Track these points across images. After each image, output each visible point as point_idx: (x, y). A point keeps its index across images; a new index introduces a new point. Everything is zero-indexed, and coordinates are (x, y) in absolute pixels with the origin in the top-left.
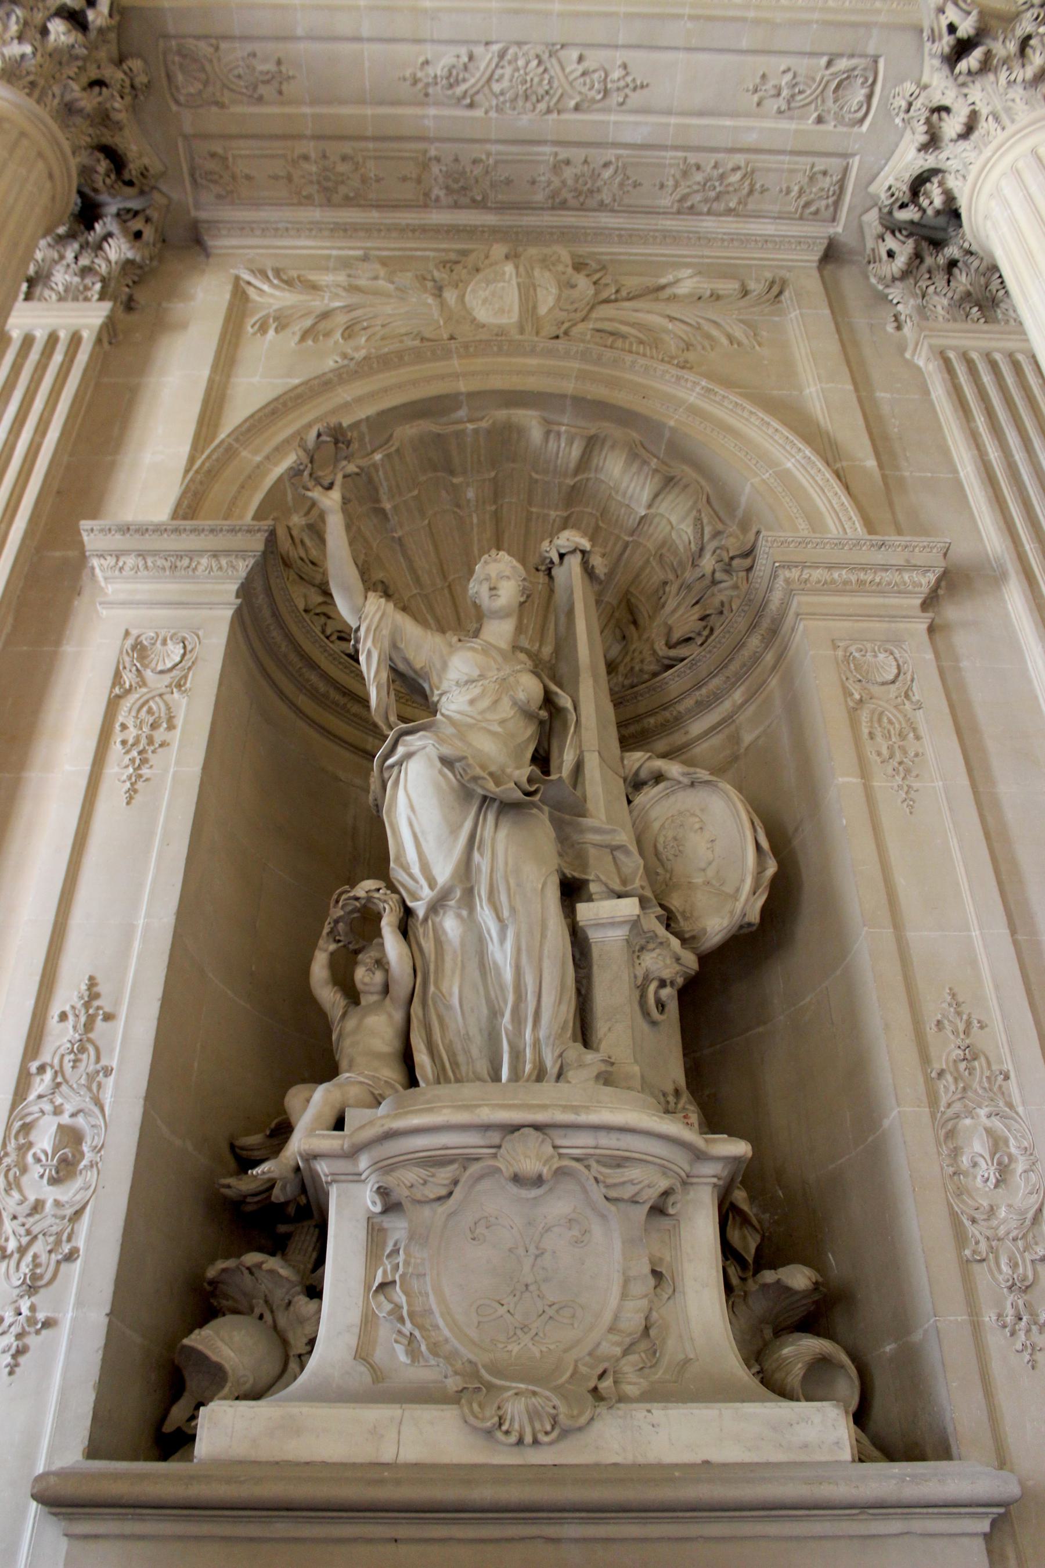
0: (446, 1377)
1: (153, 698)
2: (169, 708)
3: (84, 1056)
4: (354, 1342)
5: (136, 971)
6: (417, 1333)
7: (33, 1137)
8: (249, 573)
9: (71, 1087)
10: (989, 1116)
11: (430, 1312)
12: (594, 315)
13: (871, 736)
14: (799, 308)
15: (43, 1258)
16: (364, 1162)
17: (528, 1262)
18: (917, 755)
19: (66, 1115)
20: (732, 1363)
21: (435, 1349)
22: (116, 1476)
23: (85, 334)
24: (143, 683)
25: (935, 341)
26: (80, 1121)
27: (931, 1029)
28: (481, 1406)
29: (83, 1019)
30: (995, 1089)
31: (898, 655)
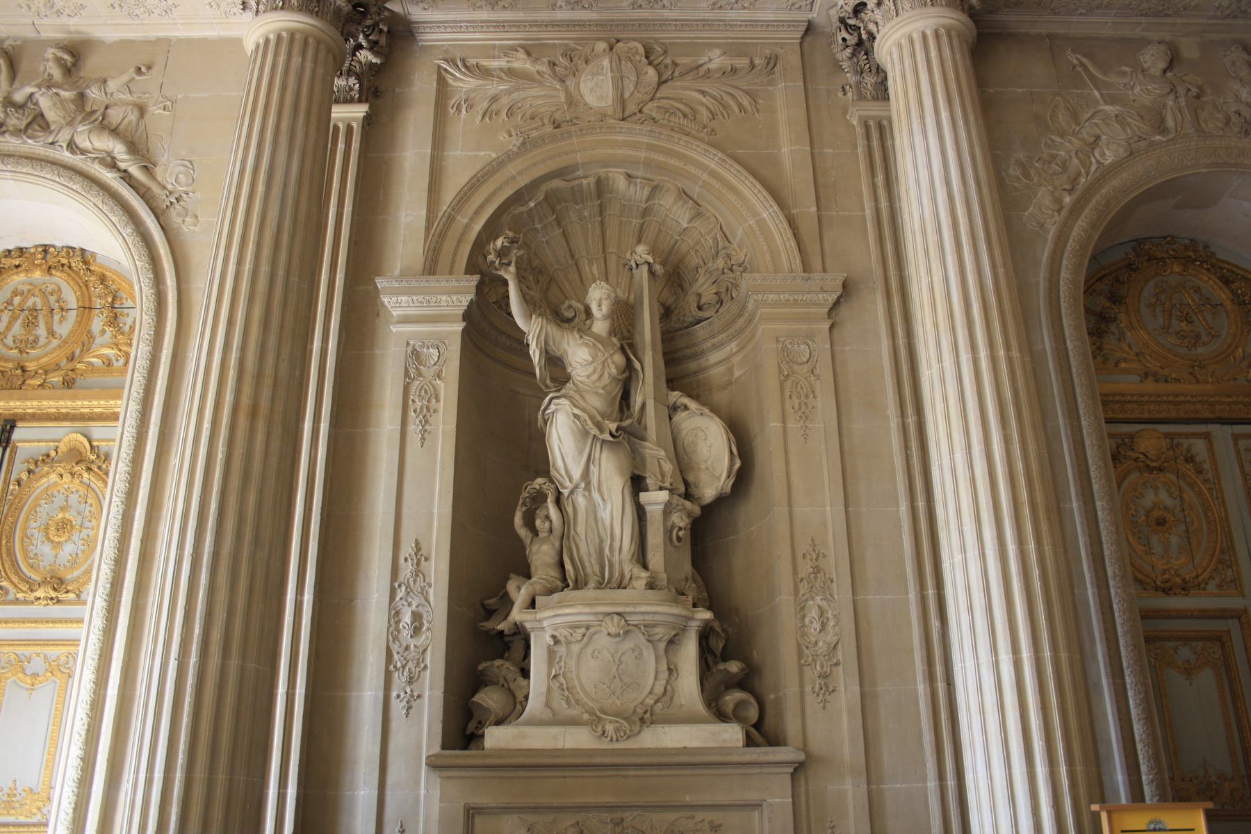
4: (544, 699)
8: (469, 307)
12: (658, 95)
13: (790, 397)
17: (614, 668)
20: (699, 706)
21: (577, 702)
22: (456, 756)
23: (354, 125)
24: (420, 375)
25: (862, 113)
27: (799, 556)
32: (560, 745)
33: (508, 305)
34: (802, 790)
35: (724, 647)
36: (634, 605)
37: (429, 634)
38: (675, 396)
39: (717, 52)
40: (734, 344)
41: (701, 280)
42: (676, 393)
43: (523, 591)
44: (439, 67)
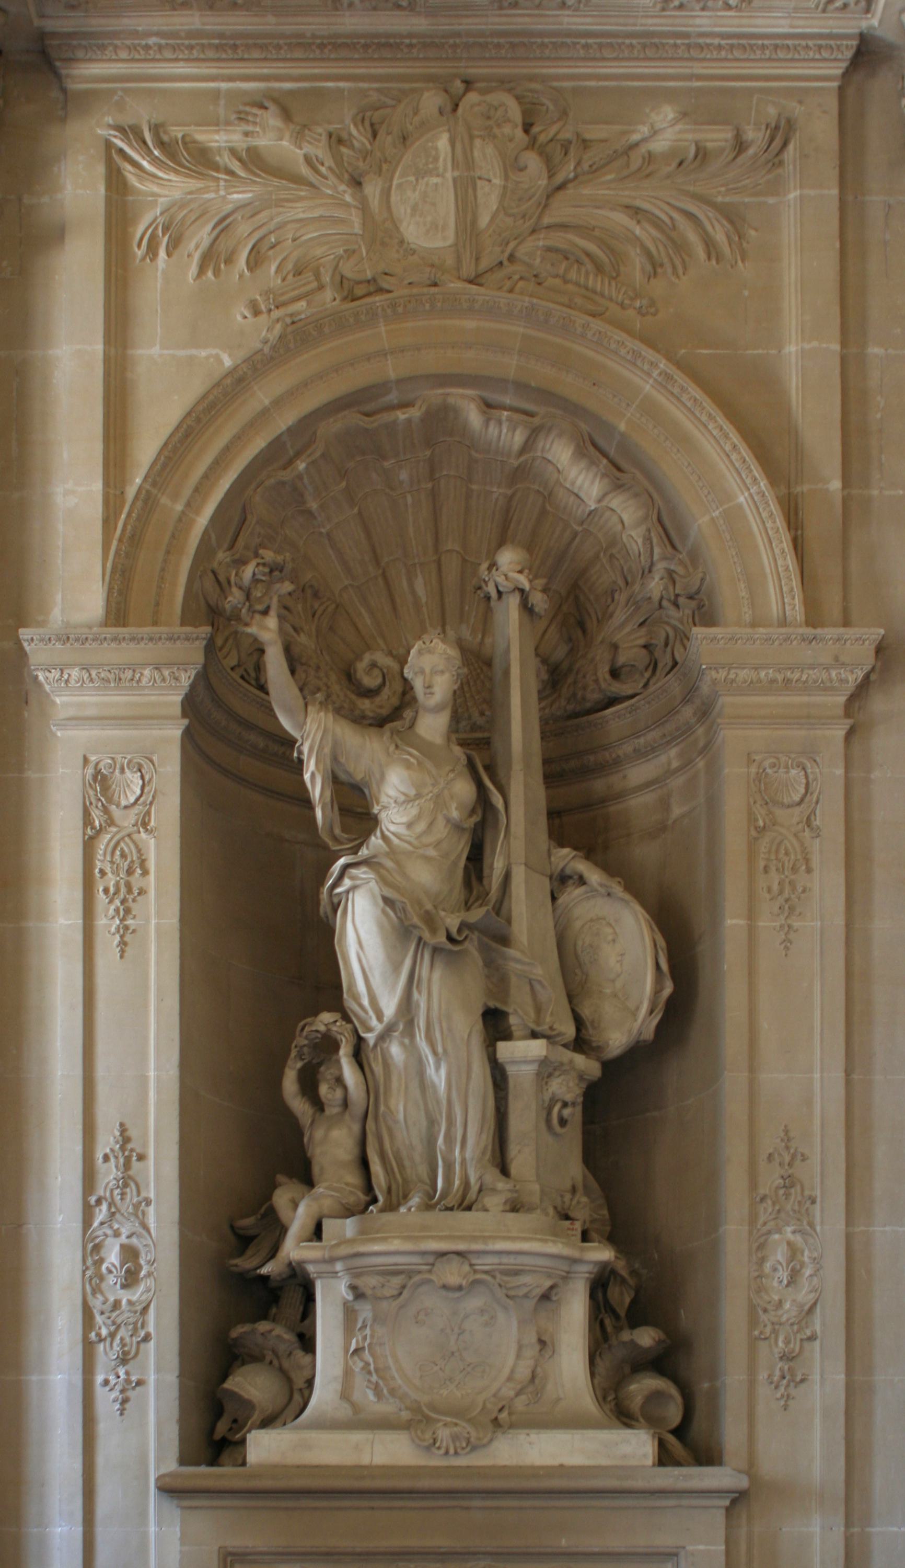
0: (400, 1410)
1: (123, 839)
2: (139, 850)
3: (128, 1190)
4: (339, 1387)
5: (157, 1120)
6: (381, 1383)
7: (103, 1253)
9: (122, 1215)
10: (794, 1232)
11: (389, 1368)
13: (766, 870)
14: (801, 187)
15: (128, 1340)
16: (339, 1266)
18: (804, 891)
19: (124, 1237)
20: (587, 1402)
21: (392, 1392)
24: (111, 822)
26: (134, 1240)
28: (422, 1432)
29: (122, 1160)
30: (803, 1211)
31: (809, 771)
32: (365, 1460)
33: (259, 668)
34: (743, 1531)
35: (634, 1302)
36: (485, 1239)
37: (150, 1282)
38: (565, 857)
39: (668, 112)
40: (673, 752)
41: (620, 616)
42: (566, 851)
43: (301, 1209)
44: (109, 145)
